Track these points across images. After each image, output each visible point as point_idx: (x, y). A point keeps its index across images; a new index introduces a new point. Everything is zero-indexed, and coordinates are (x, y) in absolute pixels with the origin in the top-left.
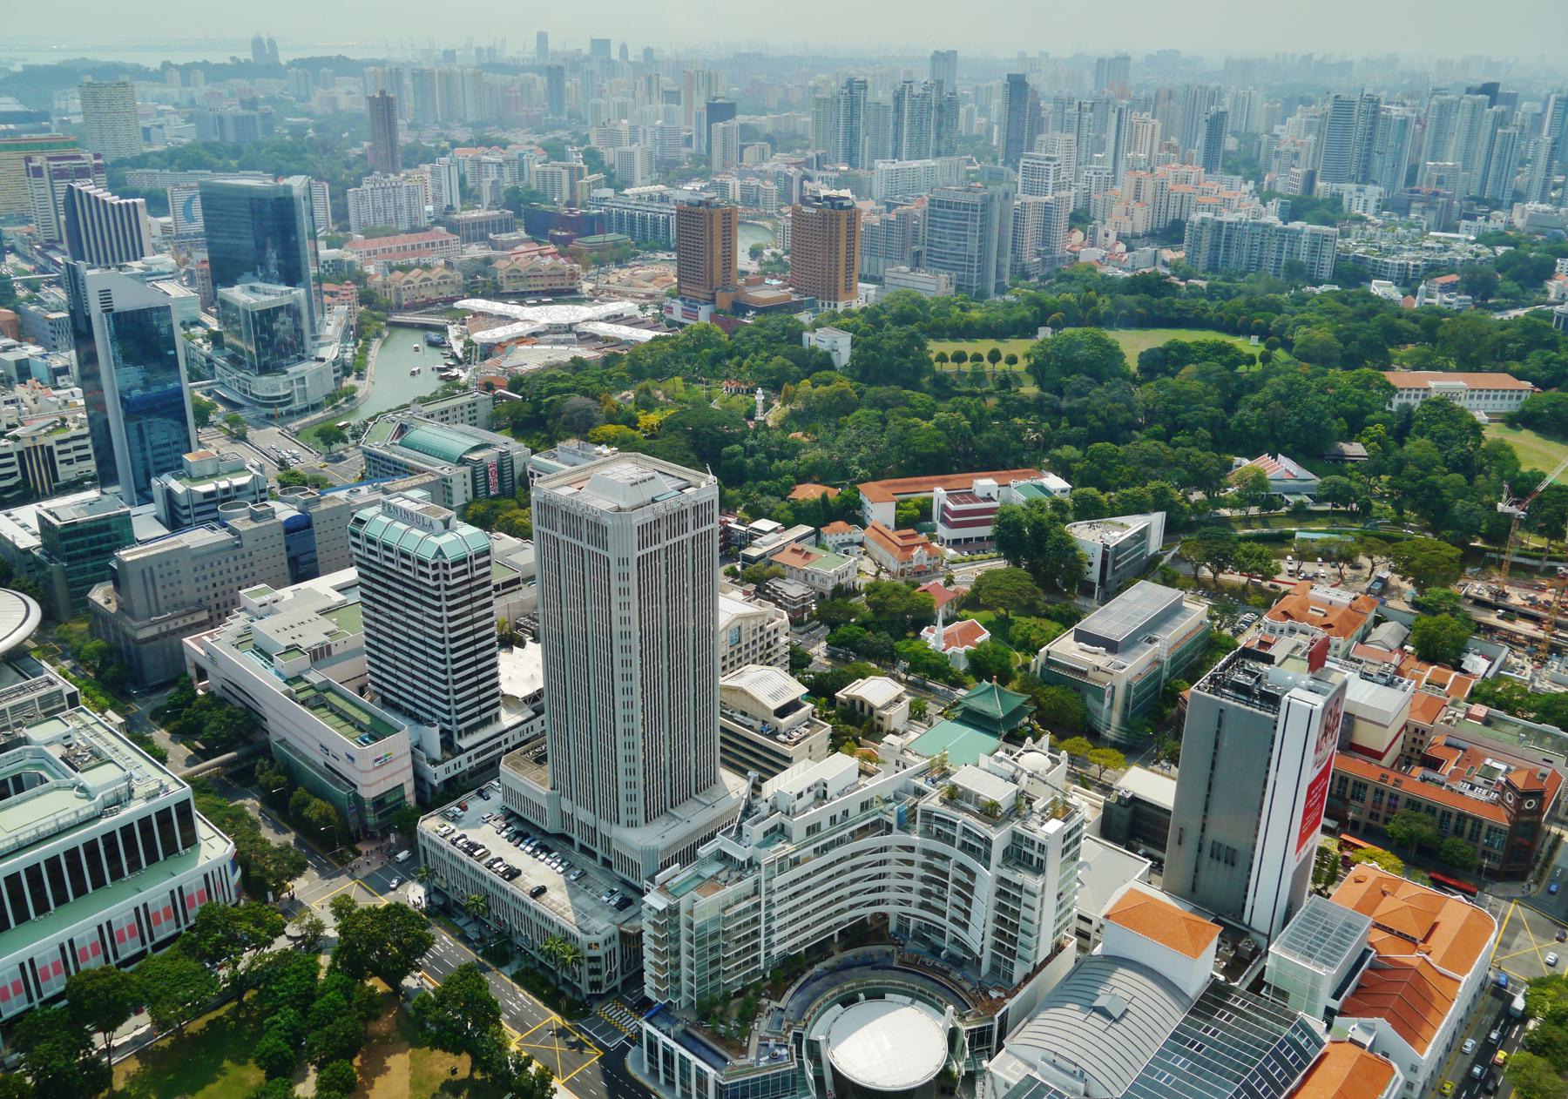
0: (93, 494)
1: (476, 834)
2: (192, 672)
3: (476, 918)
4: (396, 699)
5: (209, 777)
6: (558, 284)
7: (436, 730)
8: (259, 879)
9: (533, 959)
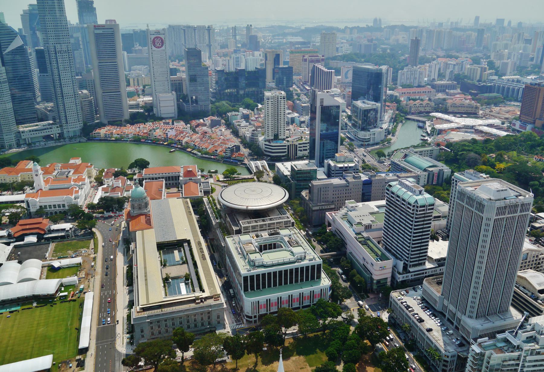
0: (307, 162)
1: (409, 301)
2: (327, 224)
3: (404, 332)
4: (390, 248)
5: (326, 258)
6: (470, 110)
7: (402, 262)
8: (336, 294)
9: (423, 353)
